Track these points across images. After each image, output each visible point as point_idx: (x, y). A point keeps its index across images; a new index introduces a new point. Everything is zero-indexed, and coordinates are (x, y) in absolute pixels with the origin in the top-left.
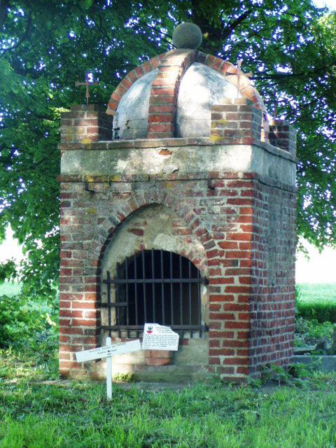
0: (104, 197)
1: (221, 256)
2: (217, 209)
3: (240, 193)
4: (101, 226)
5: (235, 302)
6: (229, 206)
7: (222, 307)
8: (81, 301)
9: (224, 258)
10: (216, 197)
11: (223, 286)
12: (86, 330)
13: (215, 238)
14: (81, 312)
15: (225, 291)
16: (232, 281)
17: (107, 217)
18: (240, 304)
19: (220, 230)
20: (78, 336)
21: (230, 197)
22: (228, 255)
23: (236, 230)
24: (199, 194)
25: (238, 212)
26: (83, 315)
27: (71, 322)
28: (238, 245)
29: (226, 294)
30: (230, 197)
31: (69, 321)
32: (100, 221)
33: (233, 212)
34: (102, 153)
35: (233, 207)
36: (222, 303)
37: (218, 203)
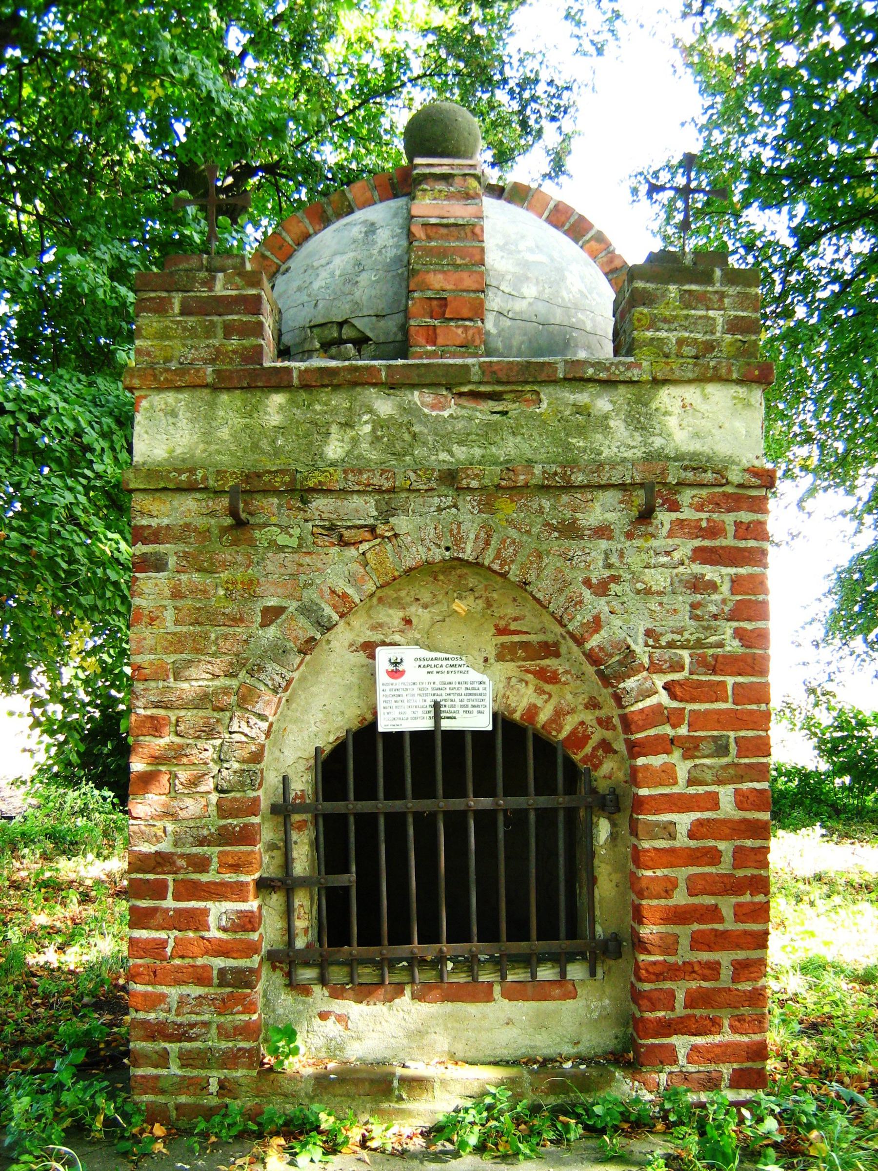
0: (282, 539)
1: (674, 727)
2: (658, 579)
3: (731, 530)
4: (272, 631)
5: (725, 867)
6: (697, 568)
7: (682, 885)
8: (204, 878)
9: (683, 731)
10: (654, 543)
11: (684, 821)
12: (222, 972)
13: (654, 668)
14: (206, 912)
15: (691, 835)
16: (713, 801)
17: (292, 606)
18: (740, 873)
19: (671, 645)
20: (196, 991)
21: (698, 543)
22: (697, 721)
23: (720, 645)
24: (603, 532)
25: (725, 588)
26: (212, 920)
27: (171, 943)
28: (730, 692)
29: (693, 844)
30: (698, 543)
31: (163, 943)
32: (271, 615)
33: (713, 587)
34: (278, 399)
35: (710, 573)
36: (682, 873)
37: (664, 559)
